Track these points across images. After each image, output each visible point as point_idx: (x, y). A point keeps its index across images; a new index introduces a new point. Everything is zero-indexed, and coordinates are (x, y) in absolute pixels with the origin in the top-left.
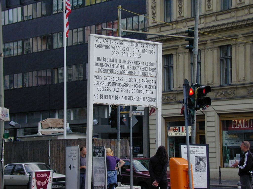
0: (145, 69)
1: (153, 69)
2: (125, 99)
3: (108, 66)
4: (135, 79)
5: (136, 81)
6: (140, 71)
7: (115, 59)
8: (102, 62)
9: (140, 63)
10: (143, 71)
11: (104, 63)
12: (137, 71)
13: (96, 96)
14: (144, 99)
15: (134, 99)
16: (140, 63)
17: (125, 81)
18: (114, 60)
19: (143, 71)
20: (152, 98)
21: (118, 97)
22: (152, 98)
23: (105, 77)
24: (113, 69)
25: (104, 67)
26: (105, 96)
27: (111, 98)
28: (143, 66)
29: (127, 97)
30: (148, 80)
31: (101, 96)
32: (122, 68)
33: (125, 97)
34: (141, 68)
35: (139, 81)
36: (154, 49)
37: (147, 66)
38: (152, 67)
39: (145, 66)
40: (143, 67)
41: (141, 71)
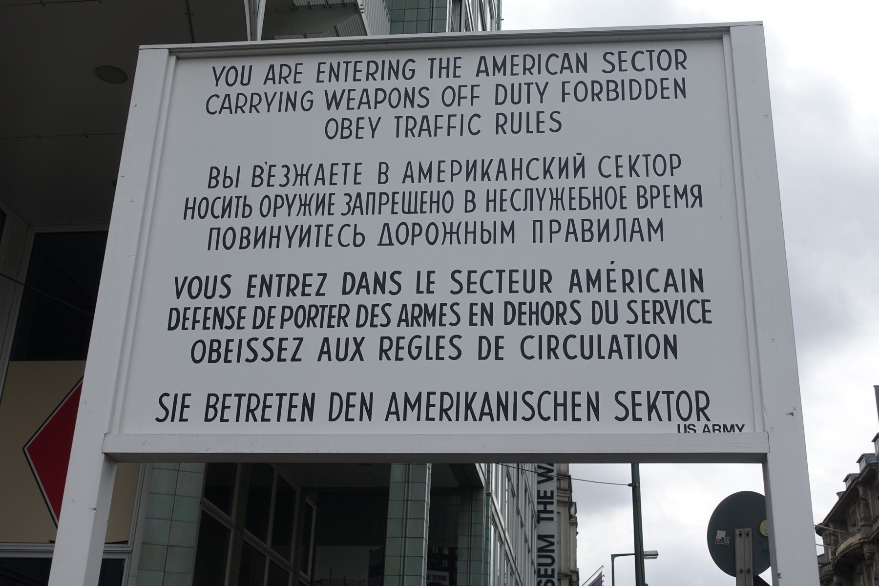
0: (599, 198)
1: (670, 191)
2: (412, 415)
3: (283, 211)
4: (506, 276)
5: (515, 287)
6: (546, 215)
7: (346, 165)
8: (245, 188)
9: (555, 169)
10: (578, 216)
11: (254, 197)
12: (523, 222)
13: (174, 409)
14: (594, 407)
15: (502, 407)
16: (555, 169)
17: (423, 287)
18: (332, 174)
19: (578, 216)
20: (668, 393)
21: (355, 400)
22: (673, 398)
23: (257, 282)
24: (325, 220)
25: (255, 221)
26: (245, 400)
27: (296, 413)
28: (577, 182)
30: (624, 271)
31: (215, 408)
32: (398, 208)
34: (557, 199)
35: (542, 283)
36: (674, 74)
37: (616, 183)
38: (660, 182)
39: (592, 179)
40: (575, 193)
41: (563, 216)
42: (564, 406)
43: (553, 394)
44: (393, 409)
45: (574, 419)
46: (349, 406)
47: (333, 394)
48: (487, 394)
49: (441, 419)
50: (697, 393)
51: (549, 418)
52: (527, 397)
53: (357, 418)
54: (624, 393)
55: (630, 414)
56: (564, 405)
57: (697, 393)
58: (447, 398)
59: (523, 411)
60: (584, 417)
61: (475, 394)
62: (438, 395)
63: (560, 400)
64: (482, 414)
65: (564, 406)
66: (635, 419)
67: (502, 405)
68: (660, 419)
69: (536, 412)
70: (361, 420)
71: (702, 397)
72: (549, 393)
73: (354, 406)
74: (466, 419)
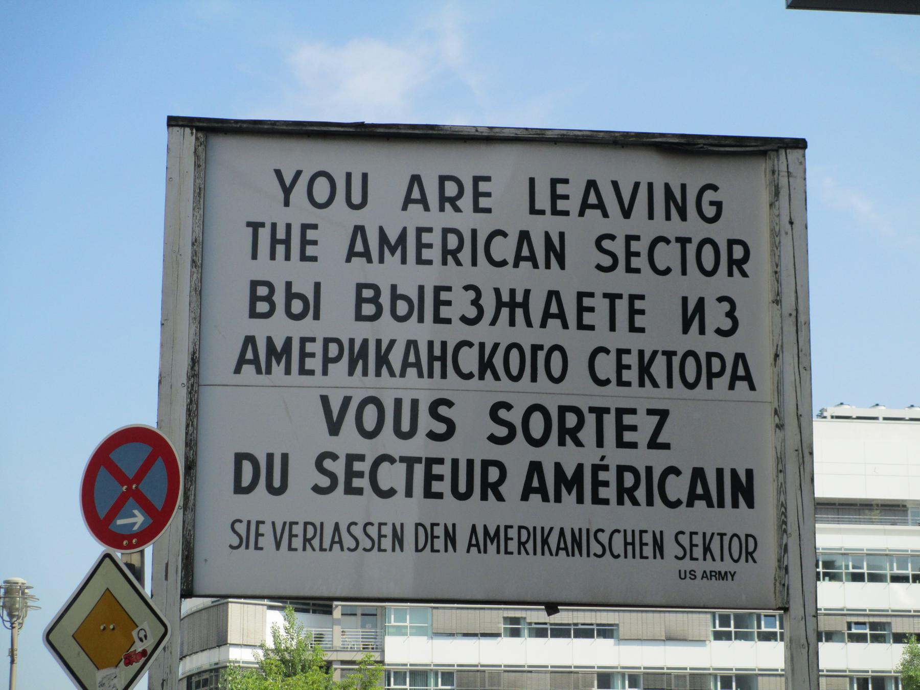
2: (492, 548)
14: (659, 546)
15: (575, 543)
20: (722, 535)
21: (439, 531)
29: (513, 533)
33: (492, 533)
42: (634, 544)
43: (622, 533)
44: (474, 542)
45: (642, 557)
46: (433, 537)
47: (417, 525)
48: (562, 530)
49: (519, 553)
50: (747, 536)
51: (618, 556)
52: (600, 535)
53: (442, 548)
54: (683, 533)
55: (687, 553)
56: (633, 544)
57: (747, 536)
58: (524, 532)
59: (596, 548)
60: (651, 555)
61: (551, 529)
62: (515, 529)
63: (629, 540)
64: (558, 548)
65: (634, 544)
66: (692, 559)
67: (577, 542)
68: (714, 560)
69: (607, 549)
70: (446, 550)
71: (751, 540)
72: (618, 531)
73: (438, 537)
74: (543, 554)
